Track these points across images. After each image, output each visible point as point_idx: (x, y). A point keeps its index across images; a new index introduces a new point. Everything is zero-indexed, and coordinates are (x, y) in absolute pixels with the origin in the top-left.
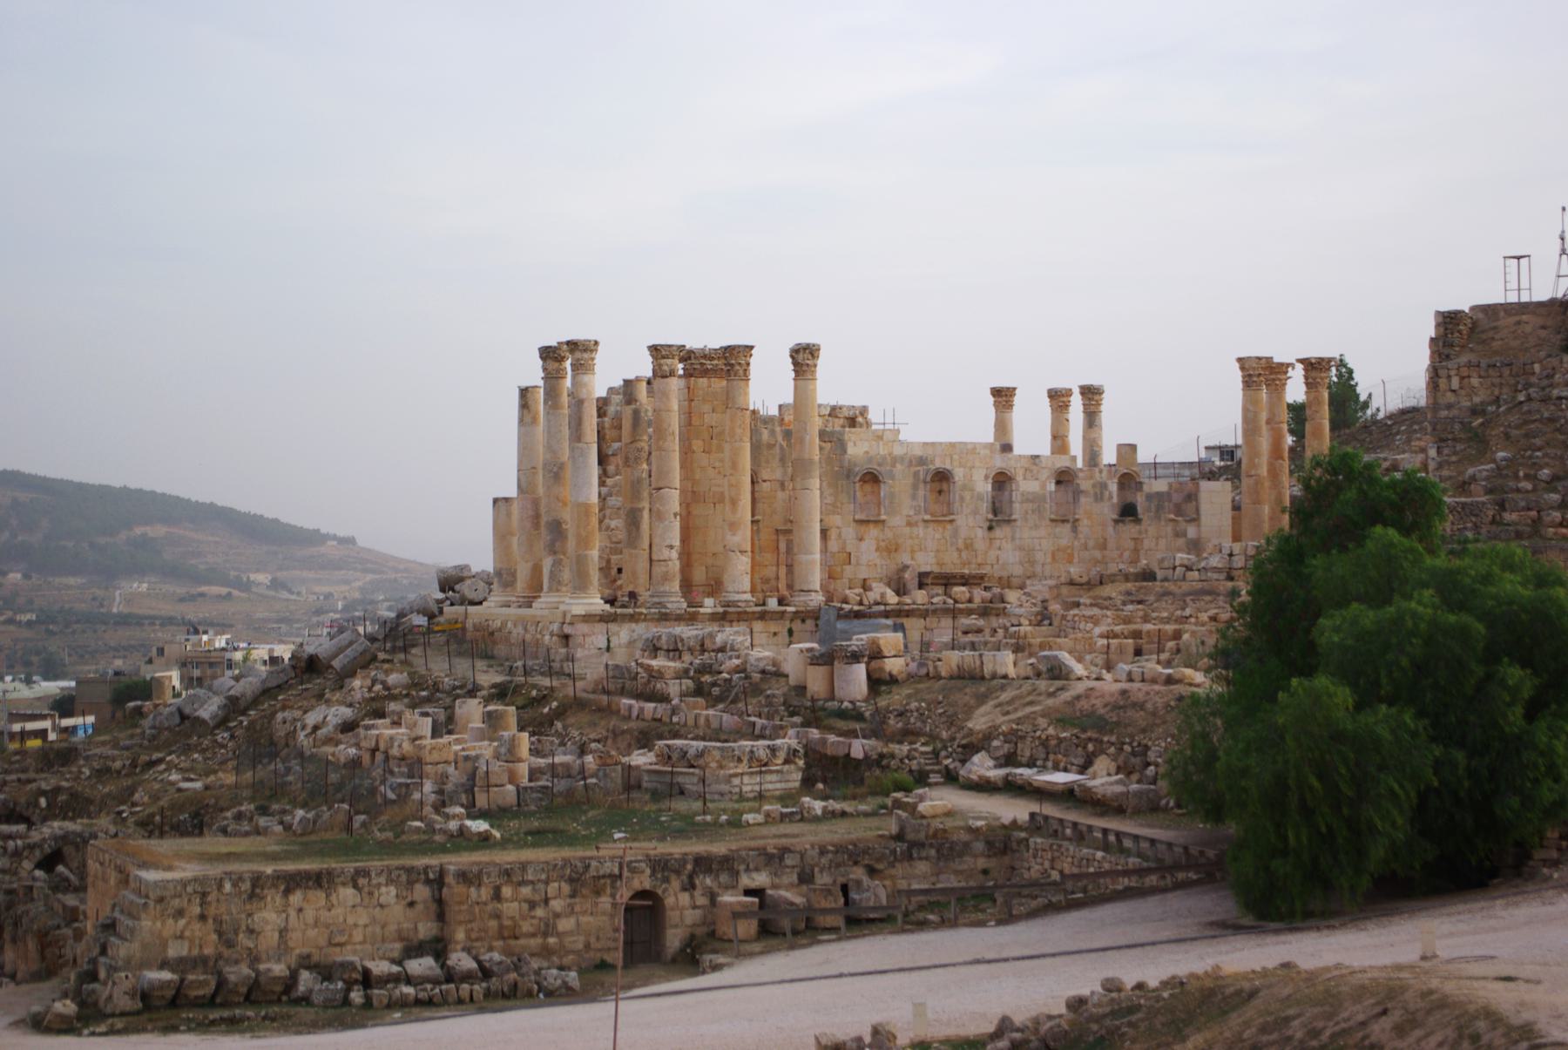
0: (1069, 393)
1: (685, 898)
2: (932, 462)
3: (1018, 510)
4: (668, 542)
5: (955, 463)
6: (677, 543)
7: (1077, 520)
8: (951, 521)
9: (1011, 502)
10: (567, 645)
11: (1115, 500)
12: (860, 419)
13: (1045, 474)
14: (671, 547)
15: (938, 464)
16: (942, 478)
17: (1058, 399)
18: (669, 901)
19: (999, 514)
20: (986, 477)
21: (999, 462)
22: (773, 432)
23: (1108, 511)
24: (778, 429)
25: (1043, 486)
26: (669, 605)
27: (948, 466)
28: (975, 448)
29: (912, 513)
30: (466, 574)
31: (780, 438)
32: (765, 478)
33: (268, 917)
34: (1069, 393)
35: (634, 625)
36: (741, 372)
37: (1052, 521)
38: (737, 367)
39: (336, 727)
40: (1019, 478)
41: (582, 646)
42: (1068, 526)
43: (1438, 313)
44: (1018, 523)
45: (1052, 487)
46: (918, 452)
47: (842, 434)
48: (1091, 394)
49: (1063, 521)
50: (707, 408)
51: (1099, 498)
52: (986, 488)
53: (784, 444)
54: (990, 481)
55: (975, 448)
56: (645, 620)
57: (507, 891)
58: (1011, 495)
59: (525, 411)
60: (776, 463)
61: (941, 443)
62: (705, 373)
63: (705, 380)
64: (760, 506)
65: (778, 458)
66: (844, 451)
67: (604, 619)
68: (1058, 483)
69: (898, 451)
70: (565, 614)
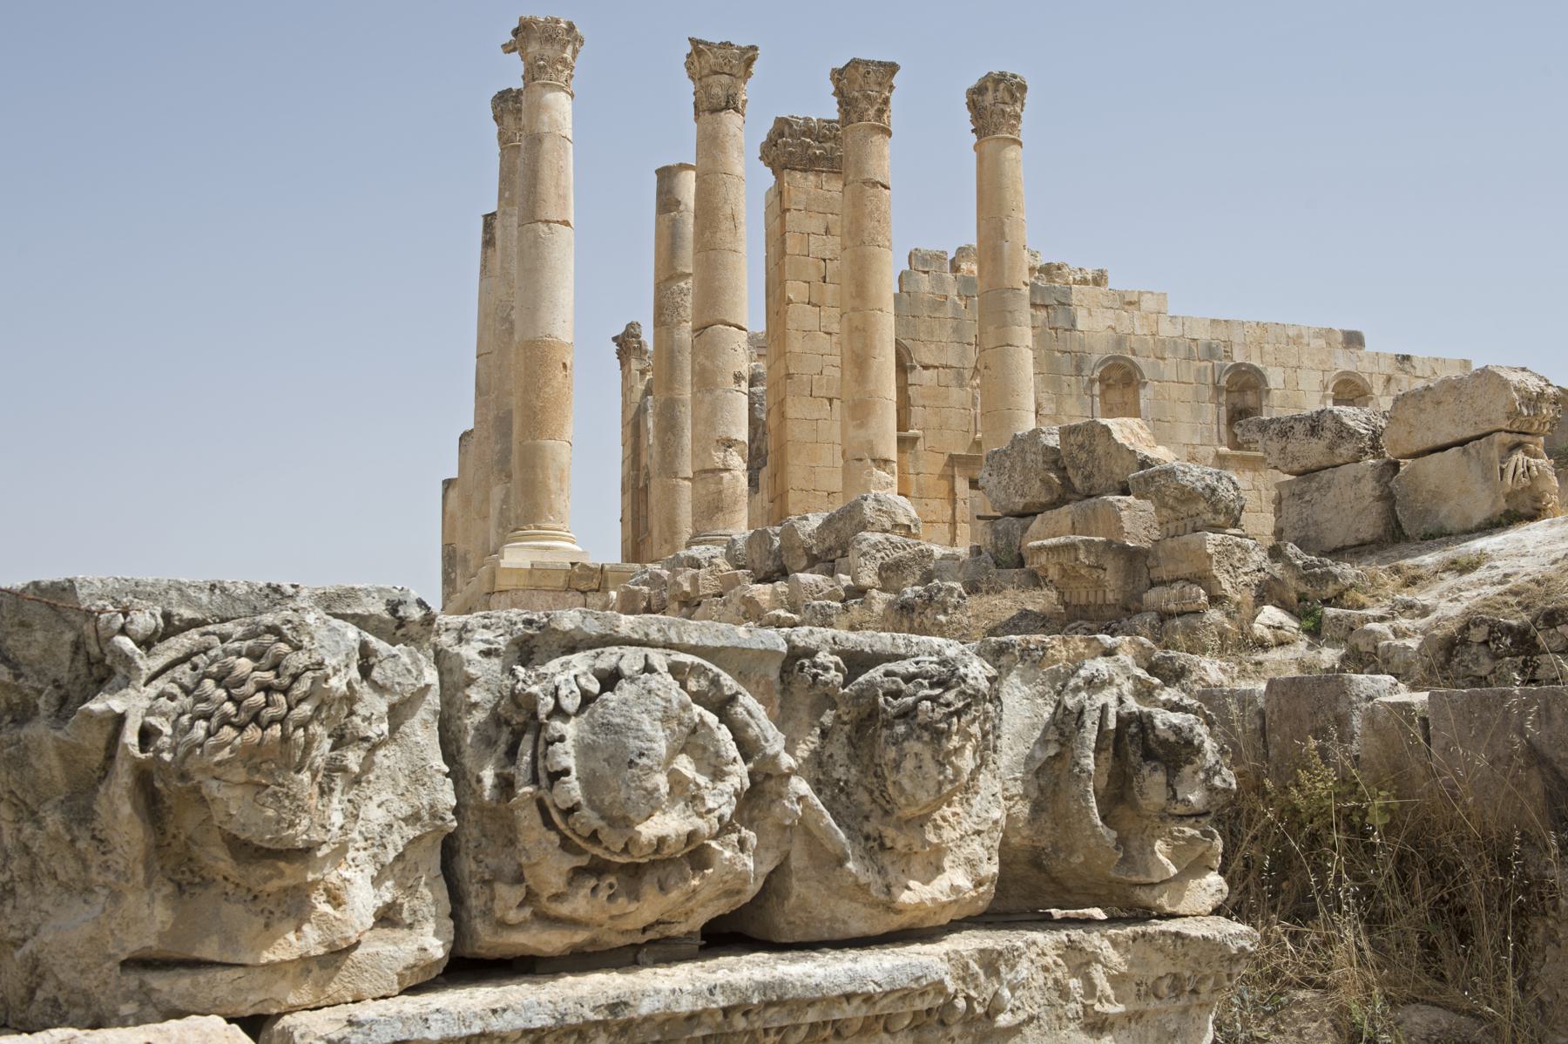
5: (1267, 358)
6: (742, 434)
14: (728, 444)
21: (1344, 362)
22: (940, 281)
24: (949, 276)
27: (1257, 363)
28: (1300, 336)
29: (1197, 440)
32: (927, 361)
46: (1203, 335)
50: (815, 224)
54: (1330, 392)
55: (1300, 336)
60: (946, 335)
63: (812, 177)
64: (917, 414)
65: (950, 323)
69: (1166, 330)
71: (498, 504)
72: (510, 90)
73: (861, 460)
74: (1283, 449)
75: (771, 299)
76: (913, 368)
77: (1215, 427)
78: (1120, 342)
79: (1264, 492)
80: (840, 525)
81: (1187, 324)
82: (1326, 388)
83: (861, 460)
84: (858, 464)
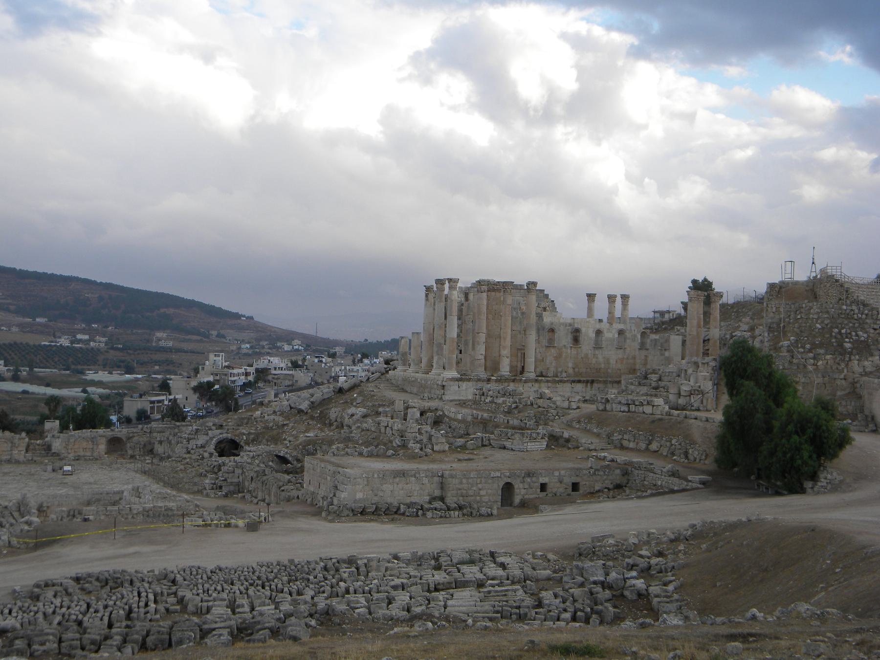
0: (615, 296)
1: (521, 486)
2: (574, 326)
3: (604, 344)
6: (484, 353)
8: (580, 347)
9: (602, 341)
10: (443, 389)
11: (639, 341)
12: (548, 308)
13: (614, 331)
15: (576, 326)
16: (577, 331)
17: (611, 298)
18: (516, 486)
19: (598, 346)
20: (593, 331)
22: (517, 313)
23: (636, 345)
25: (614, 336)
27: (580, 327)
31: (520, 315)
33: (387, 487)
34: (615, 296)
35: (468, 383)
39: (360, 416)
40: (605, 332)
43: (768, 283)
45: (616, 336)
46: (569, 321)
47: (542, 314)
48: (625, 298)
49: (620, 349)
51: (634, 340)
53: (521, 317)
57: (464, 481)
62: (494, 290)
66: (543, 320)
68: (619, 334)
69: (562, 321)
70: (443, 378)
78: (552, 324)
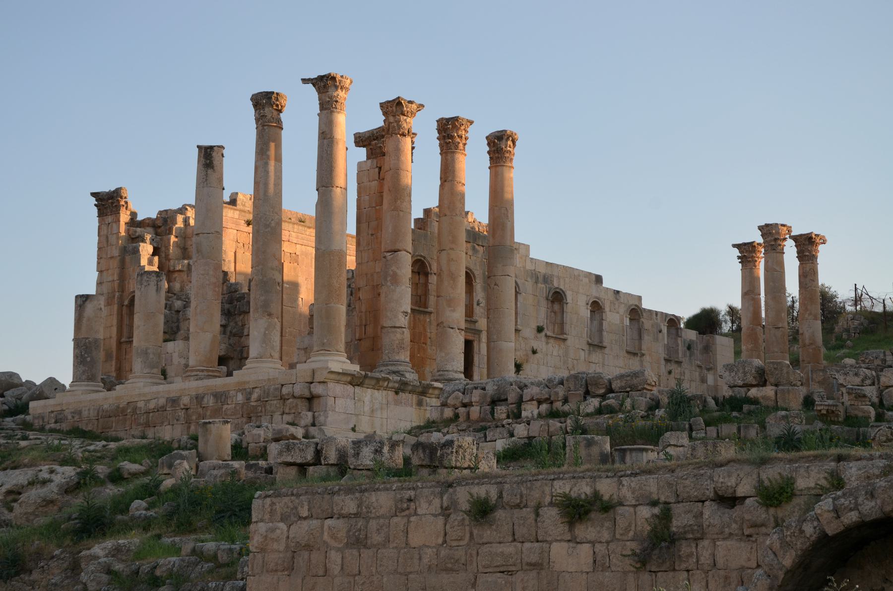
2: (552, 282)
4: (403, 309)
7: (643, 355)
8: (565, 340)
13: (622, 310)
15: (556, 285)
21: (594, 292)
25: (622, 321)
26: (407, 375)
27: (562, 287)
28: (579, 276)
30: (16, 381)
36: (461, 145)
37: (628, 352)
38: (458, 140)
39: (60, 486)
40: (607, 309)
41: (334, 411)
42: (638, 358)
44: (607, 351)
45: (627, 322)
46: (542, 270)
52: (585, 312)
56: (386, 388)
58: (601, 324)
59: (210, 171)
61: (558, 265)
67: (356, 381)
69: (529, 267)
70: (313, 372)
71: (263, 330)
72: (273, 93)
73: (452, 328)
74: (845, 379)
75: (364, 226)
76: (431, 274)
77: (545, 321)
79: (562, 358)
80: (629, 378)
81: (537, 263)
82: (587, 304)
83: (452, 328)
84: (451, 330)
